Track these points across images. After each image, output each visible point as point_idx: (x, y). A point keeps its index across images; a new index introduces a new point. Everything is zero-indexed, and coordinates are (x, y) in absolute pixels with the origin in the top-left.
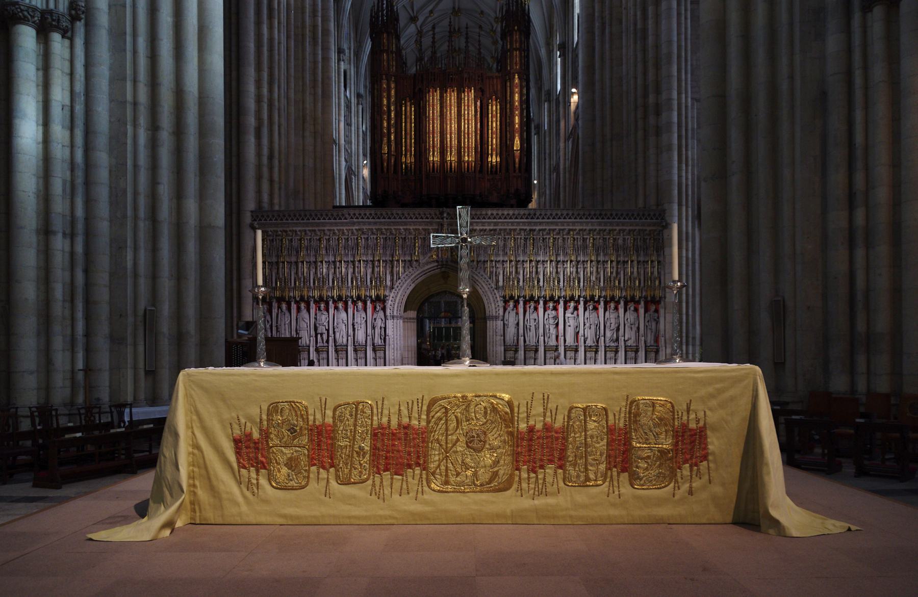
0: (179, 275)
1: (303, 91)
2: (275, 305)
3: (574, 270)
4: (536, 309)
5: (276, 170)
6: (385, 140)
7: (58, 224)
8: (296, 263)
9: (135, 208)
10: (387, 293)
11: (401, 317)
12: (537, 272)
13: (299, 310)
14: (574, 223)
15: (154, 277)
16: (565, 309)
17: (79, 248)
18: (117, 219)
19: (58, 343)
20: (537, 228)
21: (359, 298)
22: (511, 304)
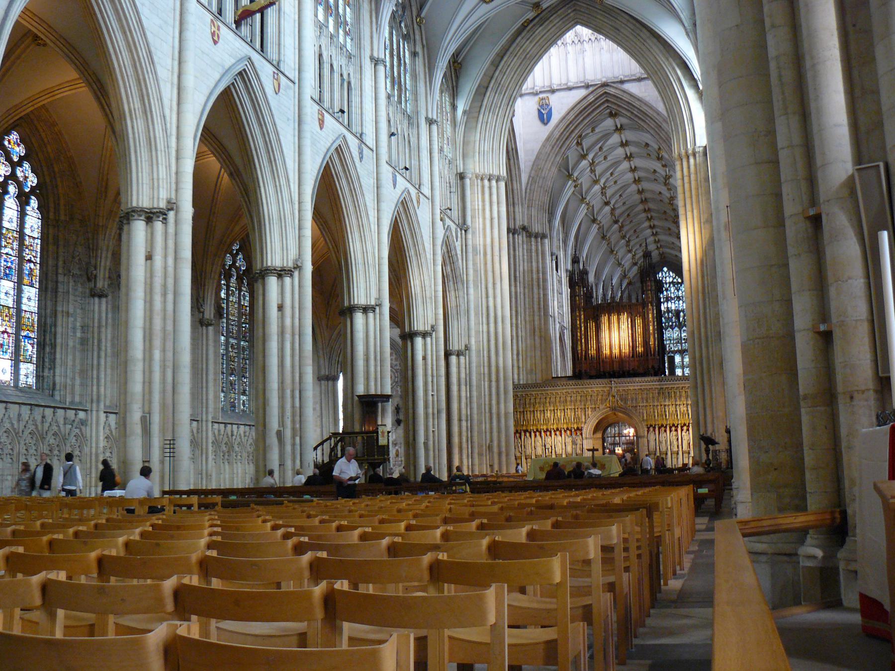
0: (499, 432)
1: (534, 315)
2: (523, 434)
3: (685, 409)
4: (665, 431)
5: (521, 361)
6: (579, 343)
7: (464, 418)
8: (534, 411)
9: (485, 409)
10: (583, 425)
11: (591, 438)
12: (665, 411)
13: (535, 436)
14: (685, 384)
15: (491, 433)
16: (682, 430)
17: (469, 425)
18: (480, 413)
19: (465, 456)
20: (665, 387)
21: (568, 429)
22: (651, 429)
